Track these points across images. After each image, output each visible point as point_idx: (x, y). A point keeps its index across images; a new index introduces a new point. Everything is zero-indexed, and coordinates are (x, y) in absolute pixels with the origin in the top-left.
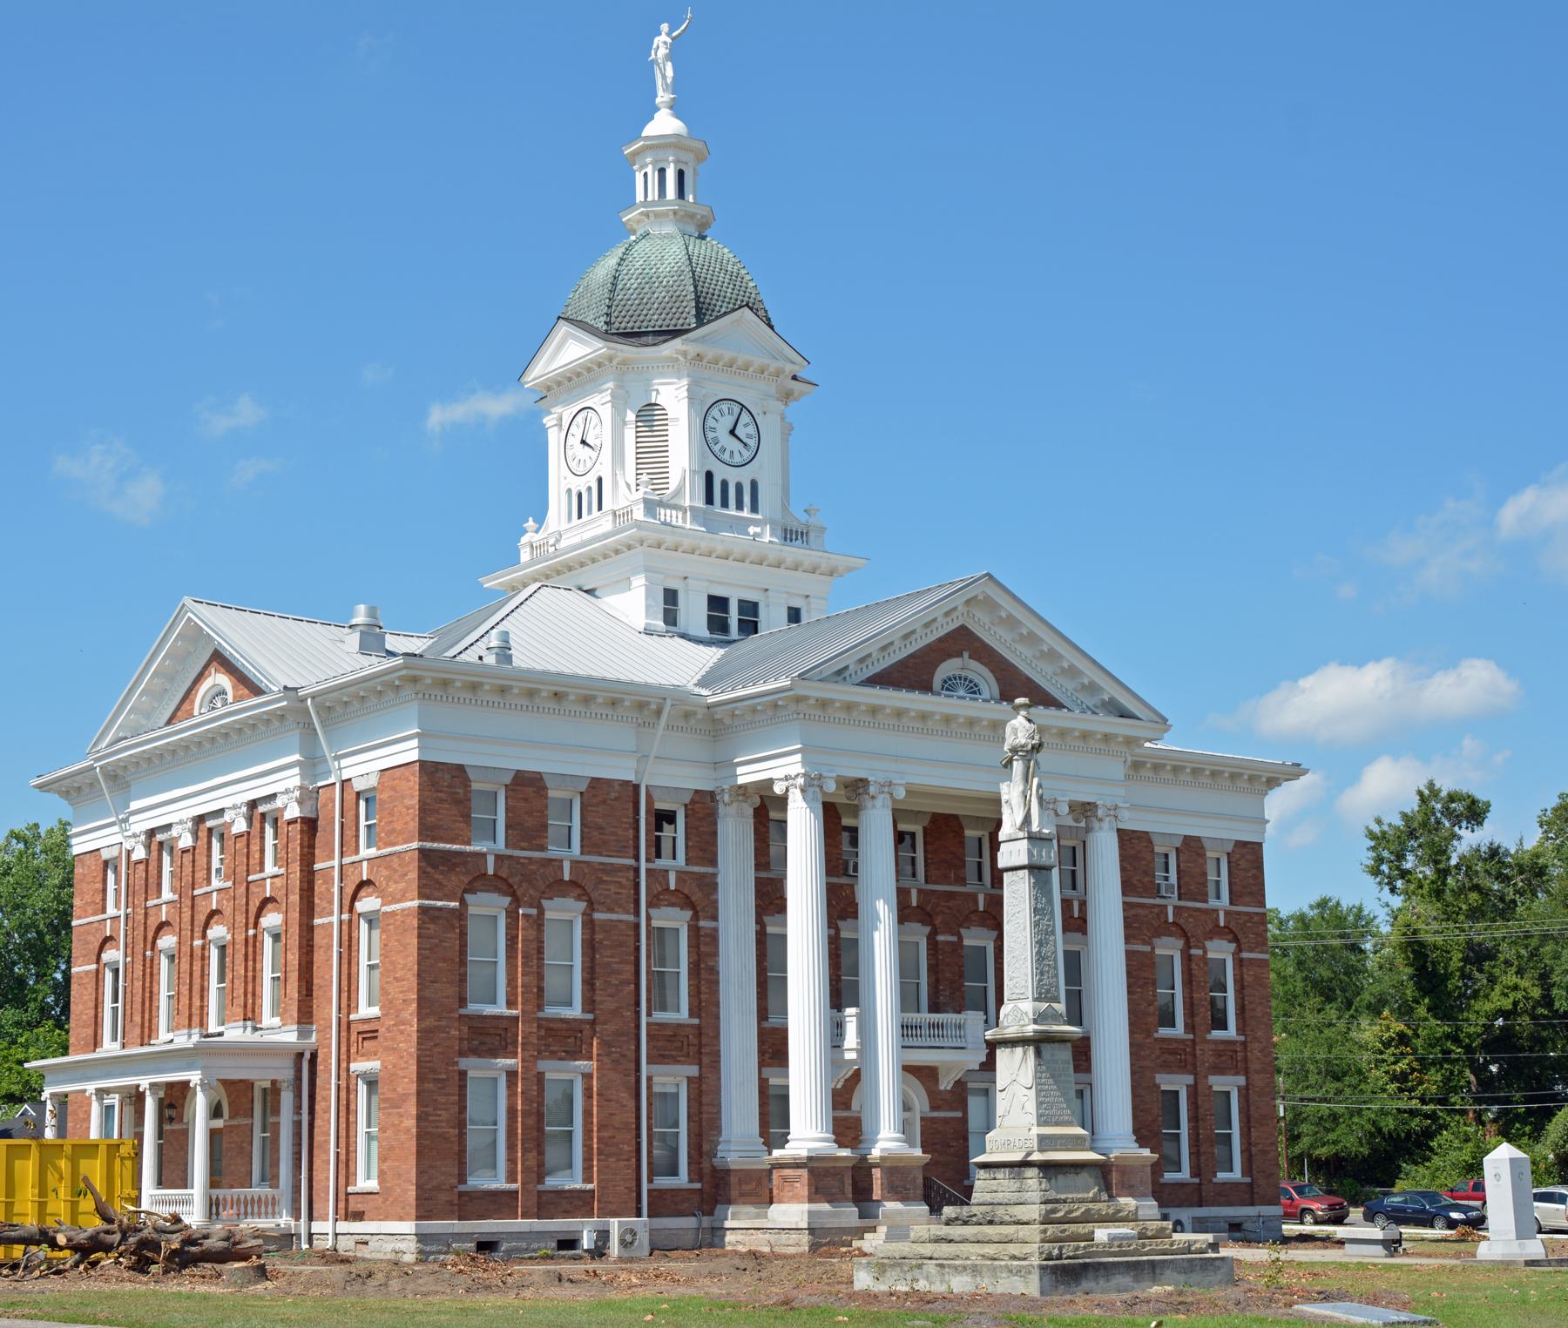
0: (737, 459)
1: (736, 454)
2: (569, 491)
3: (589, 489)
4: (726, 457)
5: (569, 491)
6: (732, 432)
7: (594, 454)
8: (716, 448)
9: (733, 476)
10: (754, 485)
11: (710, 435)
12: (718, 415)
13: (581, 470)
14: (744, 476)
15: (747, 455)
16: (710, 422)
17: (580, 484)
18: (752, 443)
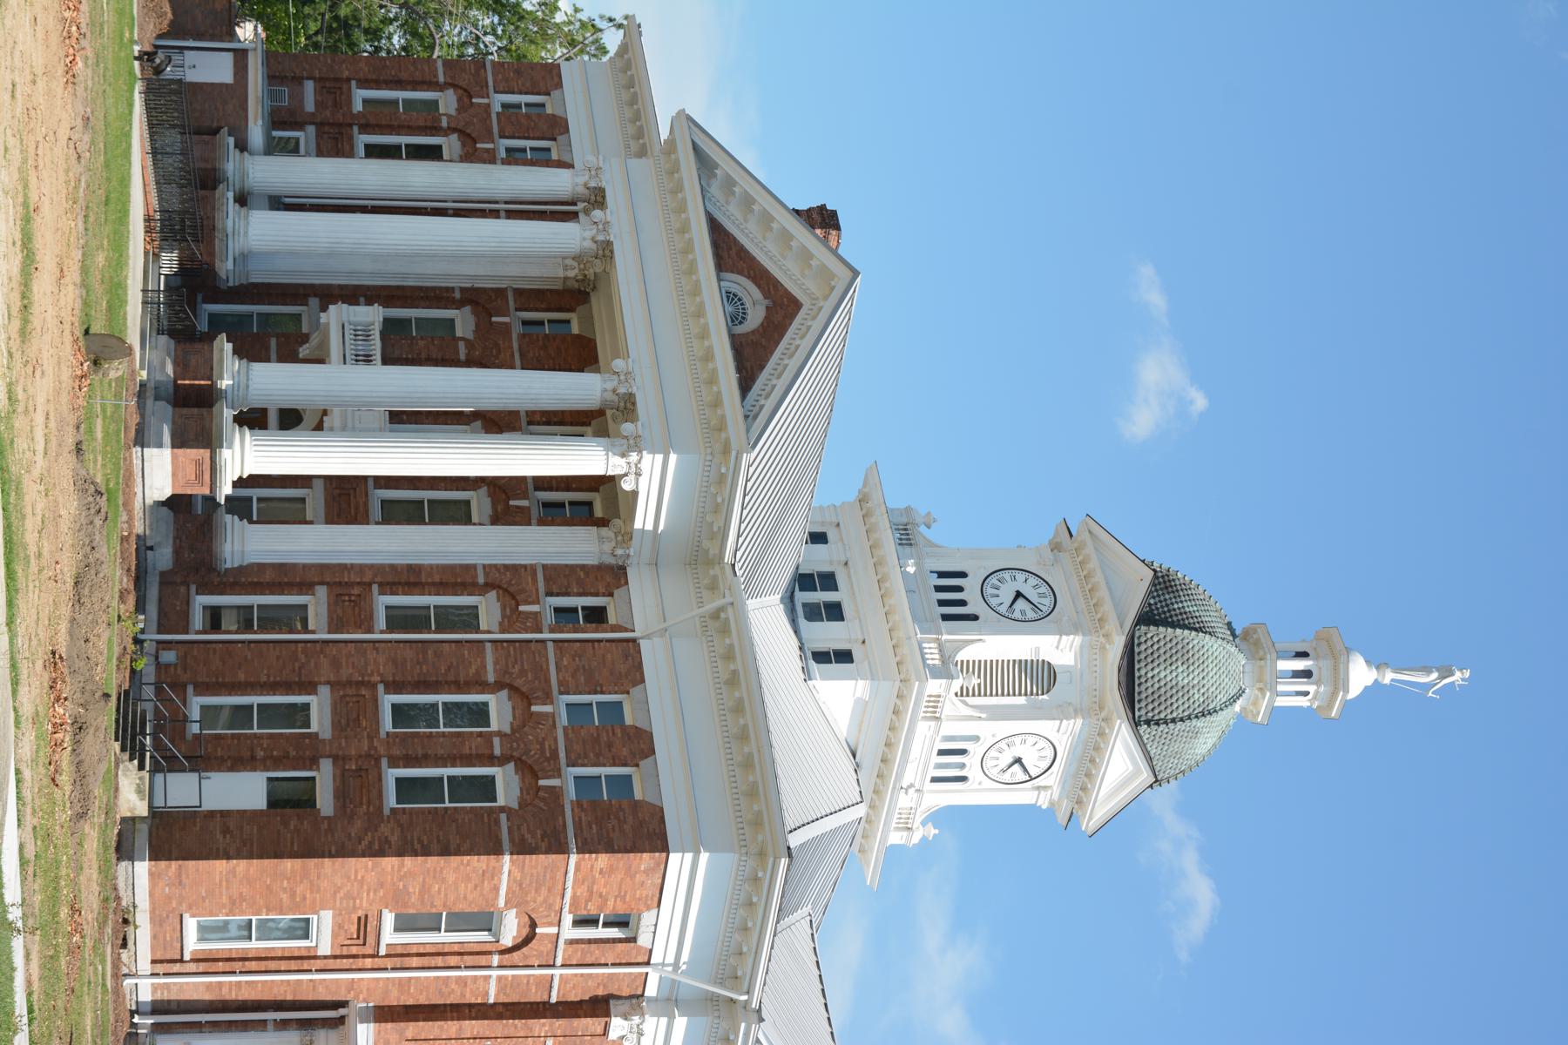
0: (988, 763)
2: (963, 575)
3: (963, 603)
4: (993, 753)
5: (963, 575)
6: (1018, 761)
7: (1003, 609)
8: (1003, 745)
9: (971, 761)
10: (963, 779)
11: (1018, 740)
13: (989, 591)
14: (973, 771)
15: (993, 773)
16: (1031, 740)
17: (971, 592)
18: (1007, 777)
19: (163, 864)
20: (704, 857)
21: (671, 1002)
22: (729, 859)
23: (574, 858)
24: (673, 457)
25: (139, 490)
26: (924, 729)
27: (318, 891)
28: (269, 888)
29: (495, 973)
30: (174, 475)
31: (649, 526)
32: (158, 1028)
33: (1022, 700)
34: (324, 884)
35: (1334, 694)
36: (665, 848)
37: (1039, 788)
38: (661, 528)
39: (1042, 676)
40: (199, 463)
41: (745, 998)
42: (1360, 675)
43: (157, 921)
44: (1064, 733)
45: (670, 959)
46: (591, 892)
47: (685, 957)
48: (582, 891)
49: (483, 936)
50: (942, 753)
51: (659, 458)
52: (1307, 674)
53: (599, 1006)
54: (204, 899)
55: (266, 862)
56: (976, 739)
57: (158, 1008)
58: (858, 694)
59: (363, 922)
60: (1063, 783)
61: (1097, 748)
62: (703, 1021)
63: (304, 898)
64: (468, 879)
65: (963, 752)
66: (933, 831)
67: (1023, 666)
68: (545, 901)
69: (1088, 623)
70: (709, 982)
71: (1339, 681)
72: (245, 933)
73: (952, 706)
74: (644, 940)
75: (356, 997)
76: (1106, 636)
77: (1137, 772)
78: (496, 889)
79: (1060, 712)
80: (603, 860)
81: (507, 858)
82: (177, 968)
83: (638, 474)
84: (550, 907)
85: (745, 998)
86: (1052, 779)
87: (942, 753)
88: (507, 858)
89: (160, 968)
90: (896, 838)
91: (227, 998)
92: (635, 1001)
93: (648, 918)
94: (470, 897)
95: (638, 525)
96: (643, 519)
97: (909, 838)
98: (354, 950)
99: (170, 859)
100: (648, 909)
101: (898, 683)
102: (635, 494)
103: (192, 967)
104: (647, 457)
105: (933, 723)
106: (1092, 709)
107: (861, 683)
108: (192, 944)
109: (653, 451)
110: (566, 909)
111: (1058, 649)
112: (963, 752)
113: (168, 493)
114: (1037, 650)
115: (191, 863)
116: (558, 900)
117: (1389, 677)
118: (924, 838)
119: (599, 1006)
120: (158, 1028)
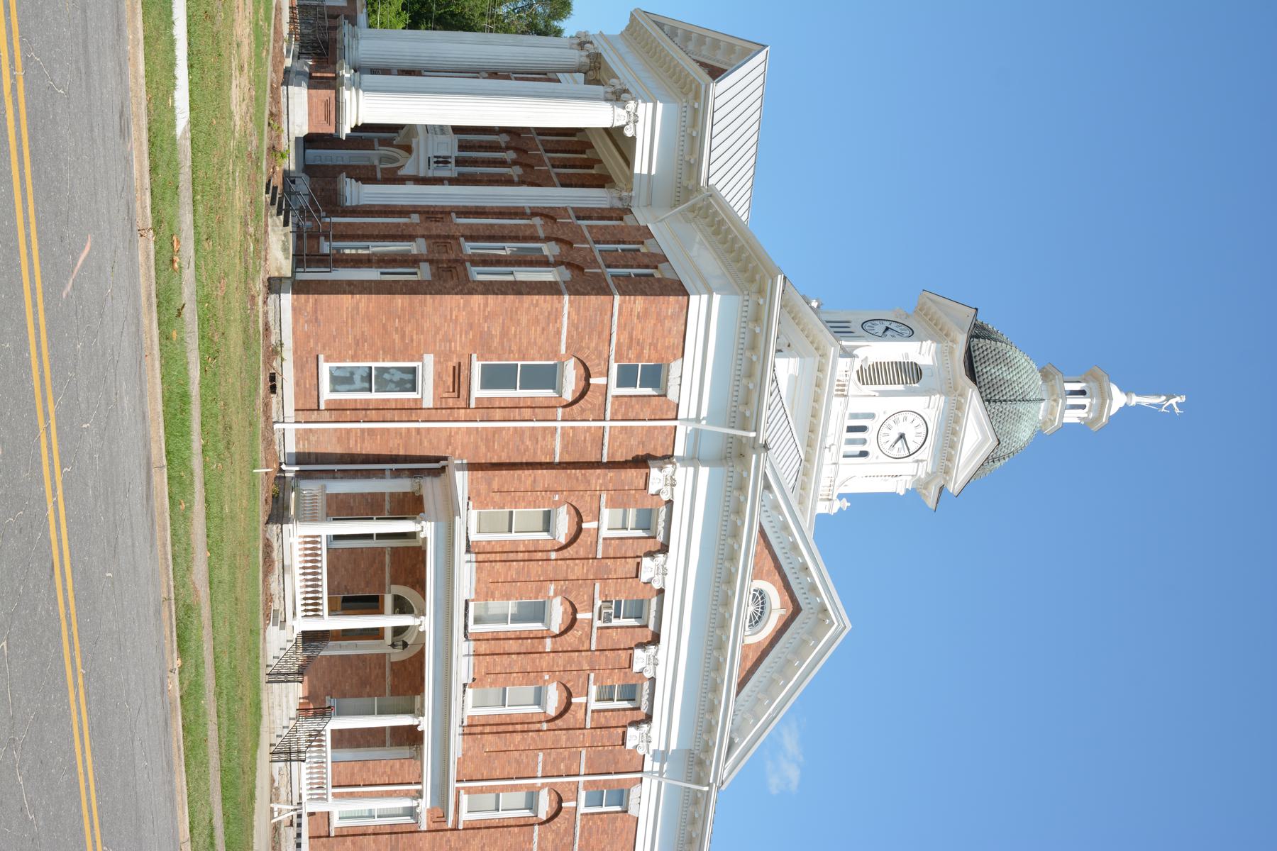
0: (882, 439)
1: (886, 439)
4: (884, 430)
8: (890, 422)
9: (870, 436)
12: (916, 423)
18: (894, 453)
19: (303, 297)
20: (717, 298)
21: (693, 459)
22: (736, 300)
23: (617, 298)
24: (660, 106)
25: (284, 126)
26: (837, 403)
27: (422, 332)
28: (384, 326)
29: (559, 425)
30: (310, 114)
31: (645, 171)
32: (301, 475)
33: (901, 387)
34: (427, 325)
35: (1102, 405)
36: (686, 293)
37: (917, 461)
38: (653, 172)
39: (913, 373)
40: (327, 104)
41: (753, 434)
42: (1119, 399)
43: (299, 366)
44: (930, 407)
45: (693, 415)
46: (631, 338)
47: (704, 413)
48: (625, 338)
49: (549, 393)
50: (851, 429)
51: (650, 105)
52: (1083, 393)
53: (641, 462)
54: (334, 338)
55: (382, 297)
56: (871, 416)
57: (301, 458)
58: (791, 372)
59: (457, 372)
60: (934, 456)
61: (954, 433)
62: (721, 471)
63: (412, 340)
64: (537, 321)
65: (863, 429)
66: (846, 504)
67: (899, 365)
68: (596, 348)
69: (938, 332)
70: (724, 427)
71: (1105, 396)
72: (367, 385)
73: (854, 387)
74: (672, 395)
75: (453, 453)
76: (953, 341)
77: (985, 439)
78: (559, 332)
79: (928, 392)
80: (640, 300)
81: (566, 297)
82: (314, 416)
83: (636, 122)
84: (600, 355)
85: (753, 434)
86: (925, 454)
87: (851, 429)
88: (566, 297)
89: (302, 416)
90: (822, 508)
91: (354, 451)
92: (668, 458)
93: (675, 367)
94: (539, 341)
95: (637, 170)
96: (641, 165)
97: (831, 507)
98: (451, 403)
99: (308, 293)
100: (675, 359)
101: (818, 358)
102: (634, 139)
103: (326, 415)
104: (642, 106)
105: (843, 399)
106: (950, 390)
107: (792, 360)
108: (326, 394)
109: (645, 101)
110: (612, 357)
111: (920, 352)
112: (863, 429)
113: (306, 132)
114: (907, 355)
115: (325, 297)
116: (606, 347)
117: (1135, 400)
118: (840, 509)
119: (641, 462)
120: (301, 475)
